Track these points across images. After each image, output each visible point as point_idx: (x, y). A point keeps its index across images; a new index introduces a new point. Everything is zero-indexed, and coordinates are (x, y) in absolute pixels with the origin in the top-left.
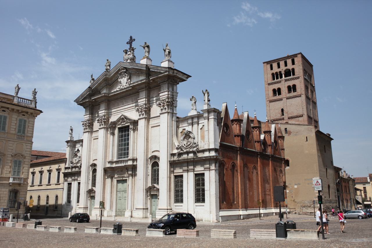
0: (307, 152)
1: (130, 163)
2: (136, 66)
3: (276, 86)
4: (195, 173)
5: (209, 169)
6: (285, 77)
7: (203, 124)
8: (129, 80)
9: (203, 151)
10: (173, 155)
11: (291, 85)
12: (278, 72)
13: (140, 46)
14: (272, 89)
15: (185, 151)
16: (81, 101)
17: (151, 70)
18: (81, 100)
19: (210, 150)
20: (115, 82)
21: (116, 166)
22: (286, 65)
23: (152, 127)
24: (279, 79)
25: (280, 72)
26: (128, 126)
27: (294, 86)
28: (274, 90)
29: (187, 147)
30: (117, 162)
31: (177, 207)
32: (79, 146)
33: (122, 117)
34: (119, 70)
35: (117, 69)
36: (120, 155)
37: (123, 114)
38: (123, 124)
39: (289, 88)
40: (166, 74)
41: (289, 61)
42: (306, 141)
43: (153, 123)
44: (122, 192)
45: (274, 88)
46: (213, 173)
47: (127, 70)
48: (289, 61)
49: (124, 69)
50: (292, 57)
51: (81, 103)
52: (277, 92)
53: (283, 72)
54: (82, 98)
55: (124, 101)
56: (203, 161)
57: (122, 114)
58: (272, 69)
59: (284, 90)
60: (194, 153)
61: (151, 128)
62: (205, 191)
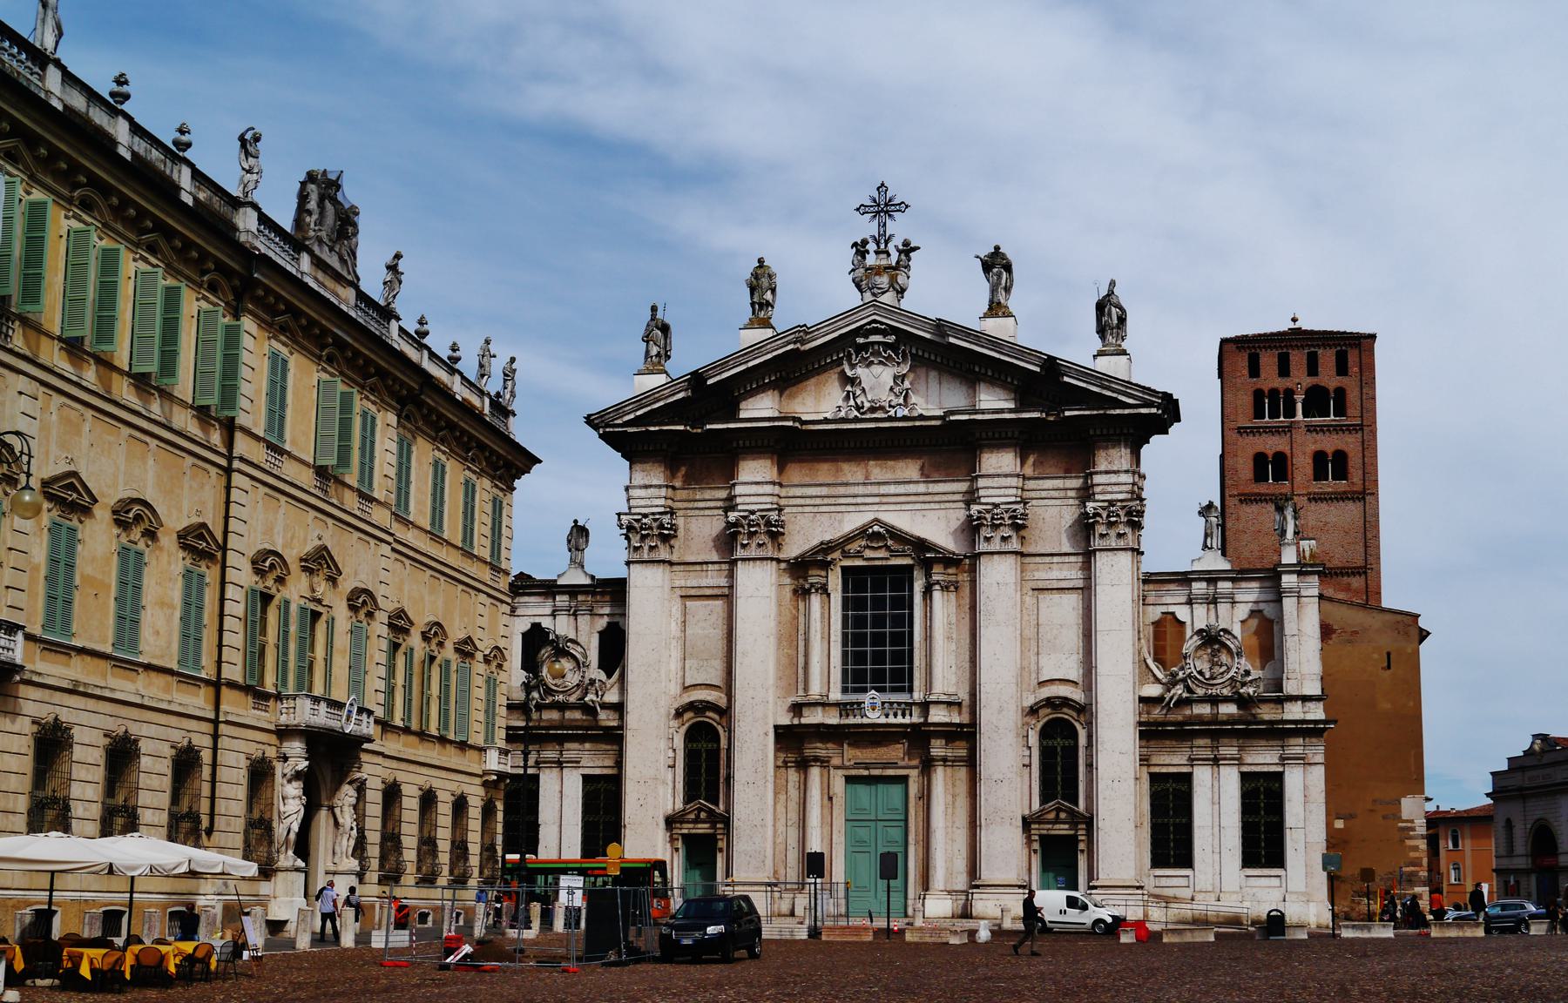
0: (1385, 705)
1: (938, 715)
2: (983, 347)
3: (1272, 445)
4: (1245, 769)
5: (1306, 763)
9: (1281, 701)
10: (1143, 700)
11: (1330, 449)
13: (977, 257)
14: (1251, 452)
15: (1200, 692)
17: (1066, 379)
18: (632, 416)
19: (1305, 699)
21: (842, 722)
22: (1313, 370)
24: (1282, 419)
25: (1290, 393)
26: (909, 568)
28: (1260, 460)
29: (1212, 682)
30: (845, 709)
31: (1164, 882)
32: (548, 611)
33: (876, 528)
34: (857, 332)
36: (855, 679)
38: (868, 553)
39: (1319, 458)
41: (1327, 358)
42: (1382, 668)
43: (1037, 575)
44: (872, 824)
45: (1260, 449)
46: (1318, 774)
48: (1327, 358)
49: (884, 333)
50: (1339, 345)
51: (630, 430)
53: (1299, 398)
54: (639, 413)
56: (1278, 733)
57: (868, 517)
58: (1254, 371)
59: (1303, 465)
60: (1243, 702)
61: (1031, 593)
62: (1288, 831)
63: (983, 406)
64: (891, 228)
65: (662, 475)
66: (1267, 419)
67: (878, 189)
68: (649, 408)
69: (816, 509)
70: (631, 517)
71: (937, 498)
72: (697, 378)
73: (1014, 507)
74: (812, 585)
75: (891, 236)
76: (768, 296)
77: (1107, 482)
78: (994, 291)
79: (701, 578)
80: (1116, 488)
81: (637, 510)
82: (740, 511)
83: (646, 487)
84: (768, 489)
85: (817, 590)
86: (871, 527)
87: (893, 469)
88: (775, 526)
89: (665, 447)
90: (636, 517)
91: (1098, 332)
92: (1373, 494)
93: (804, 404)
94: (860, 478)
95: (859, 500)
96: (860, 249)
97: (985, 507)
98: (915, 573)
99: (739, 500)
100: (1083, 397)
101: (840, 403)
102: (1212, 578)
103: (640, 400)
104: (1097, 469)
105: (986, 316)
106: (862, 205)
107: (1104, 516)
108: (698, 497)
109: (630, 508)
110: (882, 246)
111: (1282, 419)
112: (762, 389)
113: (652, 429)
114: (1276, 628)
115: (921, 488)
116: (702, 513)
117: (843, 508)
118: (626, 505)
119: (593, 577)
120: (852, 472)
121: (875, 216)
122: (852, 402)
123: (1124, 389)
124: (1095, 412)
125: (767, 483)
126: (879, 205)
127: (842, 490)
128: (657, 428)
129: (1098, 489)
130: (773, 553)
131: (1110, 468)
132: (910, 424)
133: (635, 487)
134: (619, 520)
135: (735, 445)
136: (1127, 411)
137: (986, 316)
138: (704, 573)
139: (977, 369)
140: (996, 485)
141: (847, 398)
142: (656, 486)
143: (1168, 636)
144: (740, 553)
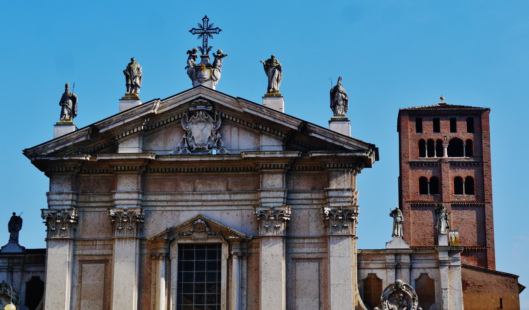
2: (264, 114)
3: (428, 174)
6: (449, 155)
7: (422, 271)
8: (219, 135)
12: (435, 141)
16: (46, 156)
17: (313, 135)
18: (53, 151)
20: (164, 126)
22: (453, 129)
23: (293, 259)
24: (435, 157)
25: (440, 142)
27: (469, 179)
33: (199, 221)
35: (184, 99)
37: (203, 213)
38: (196, 235)
39: (458, 180)
40: (358, 154)
43: (295, 250)
47: (214, 109)
50: (469, 114)
52: (429, 185)
54: (57, 149)
55: (197, 181)
58: (419, 129)
61: (291, 261)
63: (264, 149)
64: (211, 42)
65: (70, 186)
66: (427, 157)
67: (203, 19)
68: (63, 146)
69: (163, 209)
70: (50, 212)
71: (236, 203)
72: (94, 129)
73: (283, 209)
74: (161, 254)
75: (211, 47)
76: (138, 82)
77: (337, 195)
78: (270, 82)
79: (93, 249)
80: (342, 200)
81: (54, 208)
82: (117, 209)
83: (60, 193)
84: (135, 196)
85: (163, 257)
86: (196, 220)
87: (210, 185)
88: (137, 218)
89: (72, 169)
90: (53, 212)
91: (331, 107)
92: (489, 203)
93: (157, 145)
94: (190, 189)
95: (190, 203)
96: (192, 54)
97: (264, 209)
98: (222, 247)
99: (117, 202)
100: (322, 145)
101: (179, 145)
102: (397, 253)
103: (57, 141)
104: (331, 188)
105: (266, 96)
106: (194, 29)
107: (335, 216)
108: (91, 200)
109: (49, 206)
110: (205, 53)
111: (435, 157)
112: (132, 135)
113: (65, 158)
114: (436, 284)
115: (227, 197)
116: (94, 210)
117: (180, 208)
118: (47, 204)
119: (23, 248)
120: (186, 187)
121: (201, 35)
122: (186, 145)
123: (346, 141)
124: (330, 155)
125: (134, 192)
126: (203, 29)
127: (179, 197)
128: (68, 158)
129: (332, 200)
130: (137, 235)
131: (338, 187)
132: (221, 159)
133: (53, 194)
134: (43, 213)
135: (115, 169)
136: (348, 154)
137: (266, 96)
138: (94, 247)
139: (261, 127)
140: (271, 196)
141: (183, 142)
142: (66, 193)
143: (372, 288)
144: (117, 234)
